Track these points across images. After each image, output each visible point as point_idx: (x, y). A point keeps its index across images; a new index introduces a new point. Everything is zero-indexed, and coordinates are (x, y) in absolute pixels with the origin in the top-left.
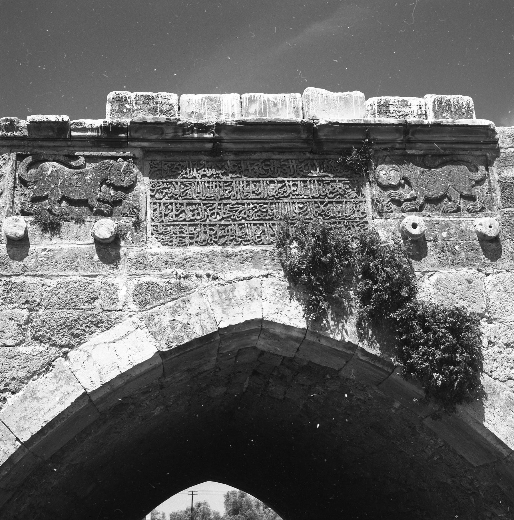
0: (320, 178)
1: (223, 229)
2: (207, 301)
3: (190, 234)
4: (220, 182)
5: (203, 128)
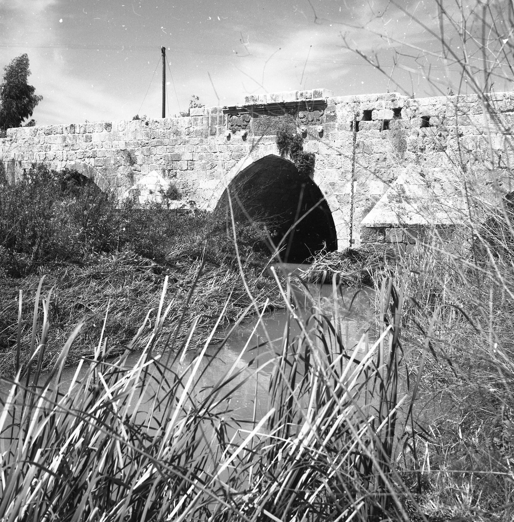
2: (262, 149)
5: (262, 105)
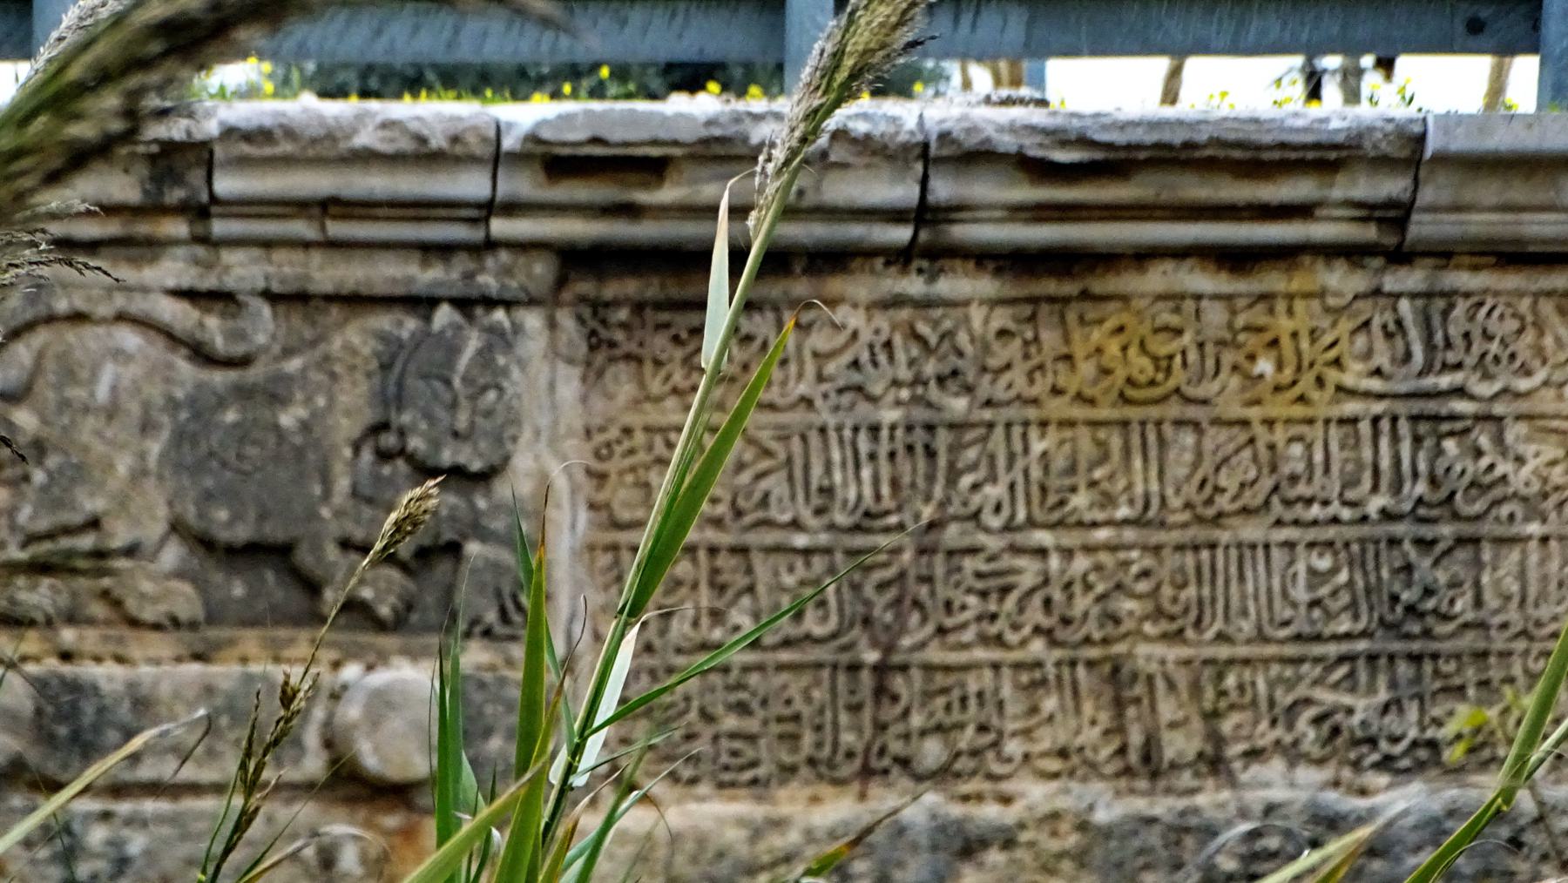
0: (1431, 406)
1: (945, 691)
3: (780, 720)
4: (930, 428)
